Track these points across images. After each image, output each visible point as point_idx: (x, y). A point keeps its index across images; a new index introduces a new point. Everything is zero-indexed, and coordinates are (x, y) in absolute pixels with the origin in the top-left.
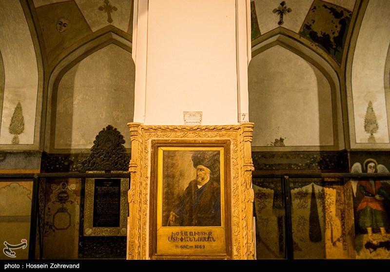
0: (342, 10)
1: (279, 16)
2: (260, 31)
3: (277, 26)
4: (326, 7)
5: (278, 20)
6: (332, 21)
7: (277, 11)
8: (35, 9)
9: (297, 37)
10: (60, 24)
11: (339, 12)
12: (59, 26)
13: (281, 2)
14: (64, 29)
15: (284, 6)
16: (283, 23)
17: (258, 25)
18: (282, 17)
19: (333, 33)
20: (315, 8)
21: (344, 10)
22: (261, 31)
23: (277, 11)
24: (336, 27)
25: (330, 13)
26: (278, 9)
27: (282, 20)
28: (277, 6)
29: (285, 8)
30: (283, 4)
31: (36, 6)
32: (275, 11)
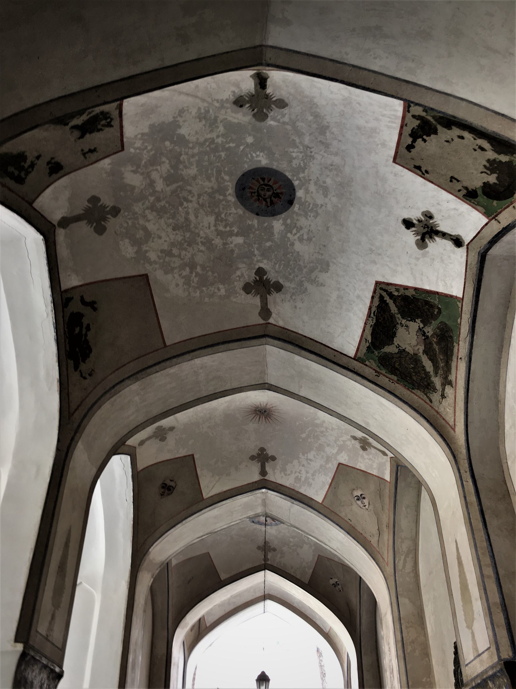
0: (409, 115)
1: (437, 238)
2: (452, 296)
3: (462, 251)
4: (410, 148)
5: (449, 244)
6: (447, 141)
7: (423, 239)
8: (321, 504)
9: (495, 228)
10: (358, 499)
11: (416, 123)
12: (359, 502)
13: (403, 227)
14: (366, 501)
15: (415, 222)
16: (458, 235)
17: (437, 293)
18: (444, 235)
19: (482, 149)
20: (419, 168)
21: (409, 111)
22: (454, 294)
23: (423, 239)
24: (462, 138)
25: (425, 141)
26: (419, 237)
27: (451, 235)
28: (410, 237)
29: (419, 221)
30: (408, 224)
31: (320, 501)
32: (422, 244)
